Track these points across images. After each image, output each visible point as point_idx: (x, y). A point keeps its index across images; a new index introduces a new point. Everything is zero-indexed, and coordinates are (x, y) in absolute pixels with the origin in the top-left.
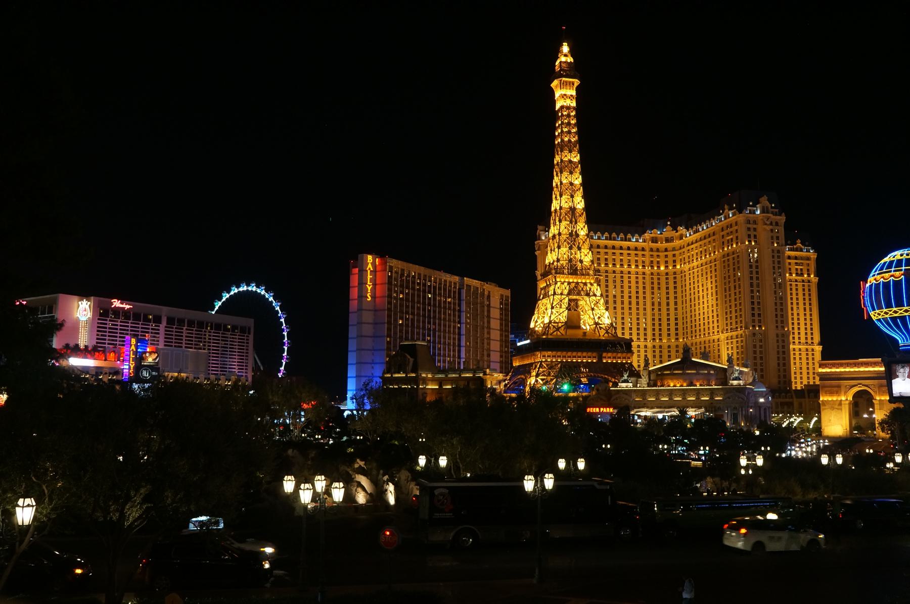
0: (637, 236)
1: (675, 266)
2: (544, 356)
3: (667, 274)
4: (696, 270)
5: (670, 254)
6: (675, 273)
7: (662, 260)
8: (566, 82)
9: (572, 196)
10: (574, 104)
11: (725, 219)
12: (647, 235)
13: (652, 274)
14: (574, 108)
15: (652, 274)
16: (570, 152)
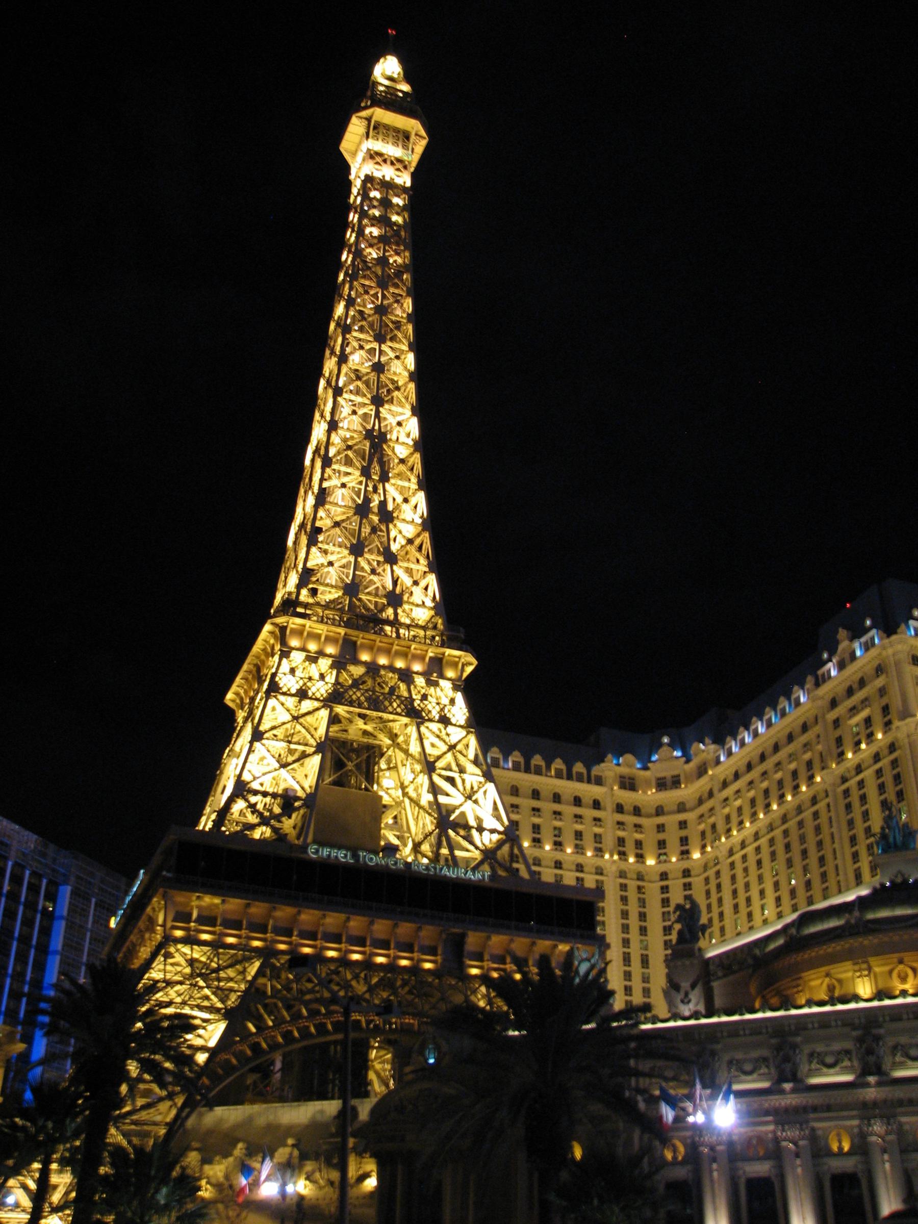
0: (579, 767)
1: (685, 853)
2: (183, 917)
3: (664, 876)
4: (750, 849)
5: (671, 820)
6: (686, 873)
7: (649, 838)
8: (387, 127)
9: (378, 401)
10: (405, 179)
11: (841, 666)
12: (611, 768)
13: (622, 874)
14: (404, 189)
15: (622, 874)
16: (383, 283)
